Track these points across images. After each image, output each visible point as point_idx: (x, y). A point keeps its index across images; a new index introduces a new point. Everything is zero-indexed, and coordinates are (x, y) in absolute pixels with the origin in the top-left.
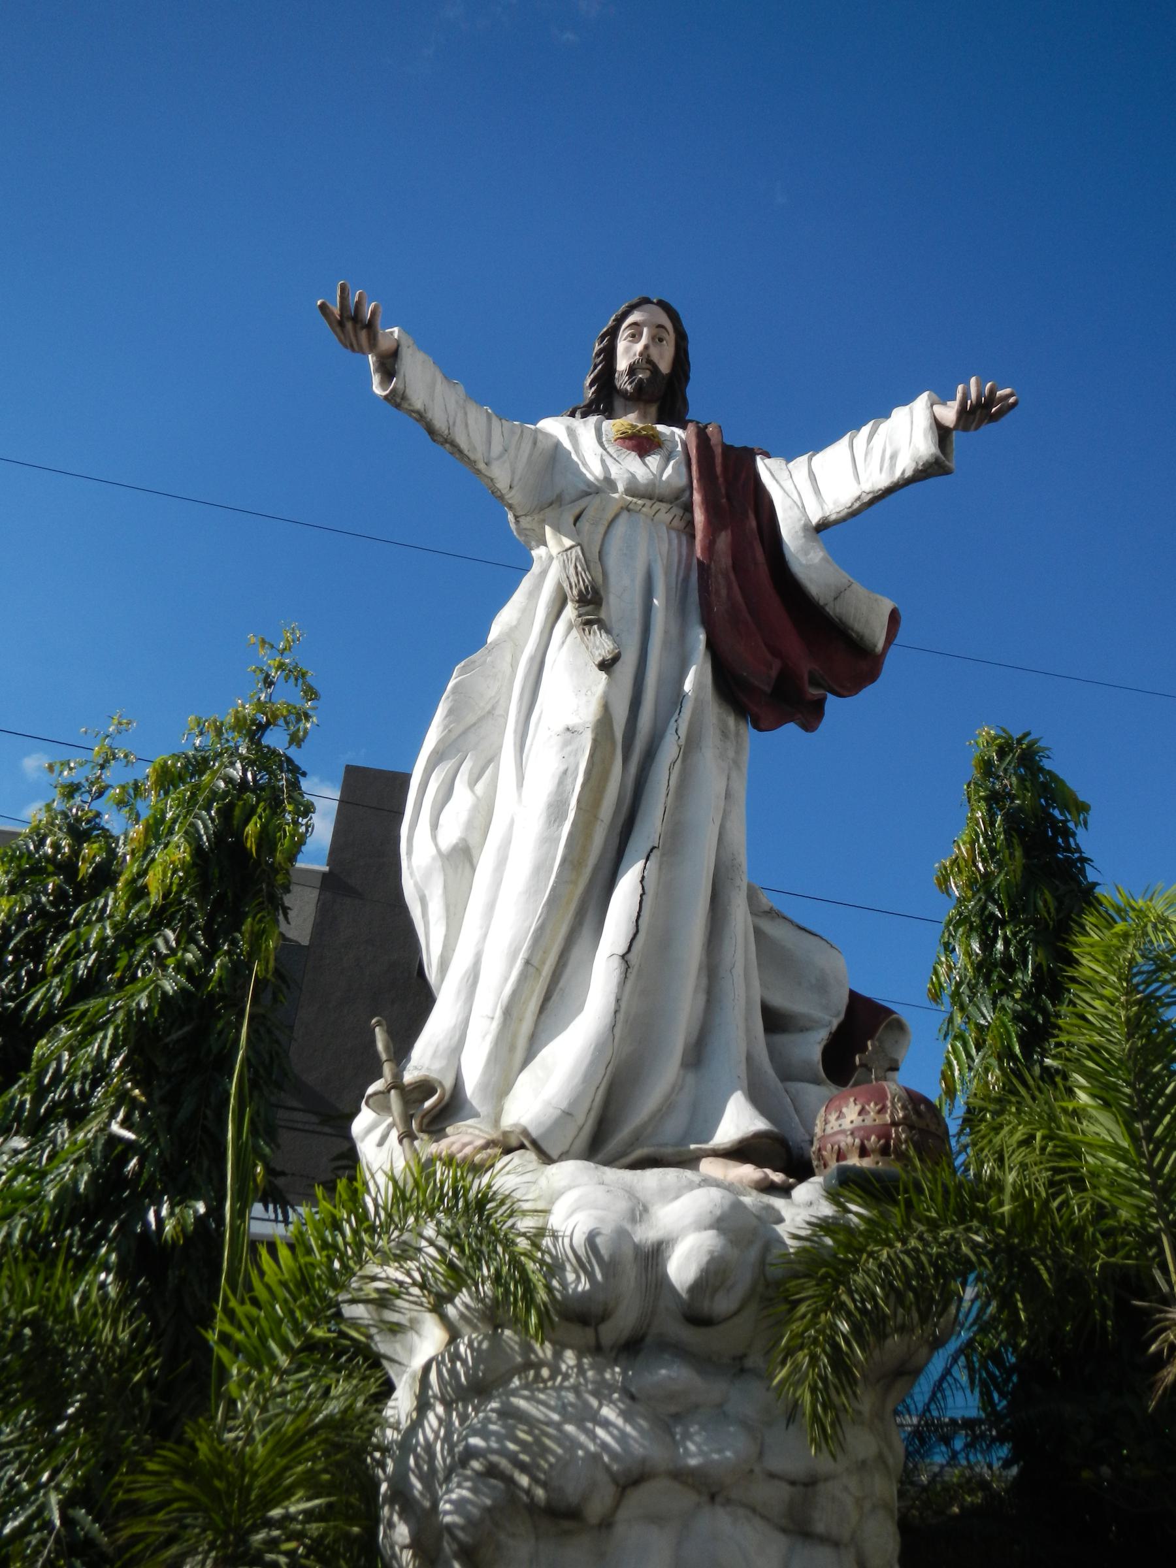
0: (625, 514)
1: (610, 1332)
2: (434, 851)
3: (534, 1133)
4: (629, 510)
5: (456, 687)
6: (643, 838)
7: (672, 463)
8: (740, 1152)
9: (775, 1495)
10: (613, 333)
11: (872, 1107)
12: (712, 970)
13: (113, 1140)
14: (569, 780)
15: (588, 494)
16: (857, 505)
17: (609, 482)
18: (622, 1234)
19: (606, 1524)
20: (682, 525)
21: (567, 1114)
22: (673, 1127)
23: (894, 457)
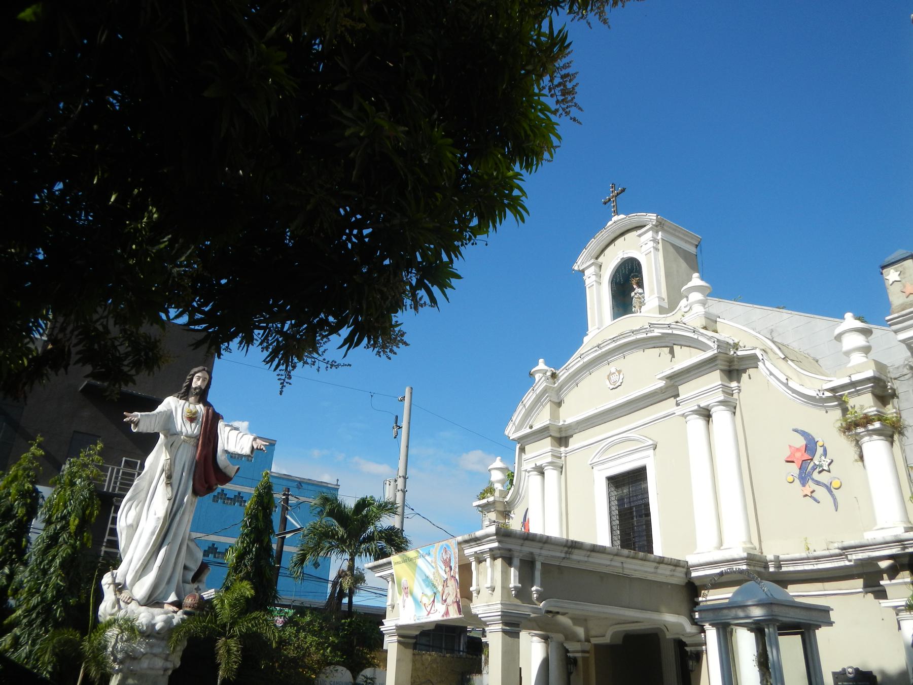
0: (183, 443)
1: (145, 635)
2: (125, 525)
3: (139, 600)
4: (184, 441)
5: (136, 485)
6: (167, 541)
7: (198, 426)
8: (173, 604)
9: (164, 656)
10: (193, 375)
11: (193, 600)
12: (175, 563)
13: (58, 584)
15: (175, 434)
17: (182, 432)
18: (150, 622)
19: (140, 659)
20: (195, 445)
21: (145, 597)
22: (162, 596)
23: (242, 449)
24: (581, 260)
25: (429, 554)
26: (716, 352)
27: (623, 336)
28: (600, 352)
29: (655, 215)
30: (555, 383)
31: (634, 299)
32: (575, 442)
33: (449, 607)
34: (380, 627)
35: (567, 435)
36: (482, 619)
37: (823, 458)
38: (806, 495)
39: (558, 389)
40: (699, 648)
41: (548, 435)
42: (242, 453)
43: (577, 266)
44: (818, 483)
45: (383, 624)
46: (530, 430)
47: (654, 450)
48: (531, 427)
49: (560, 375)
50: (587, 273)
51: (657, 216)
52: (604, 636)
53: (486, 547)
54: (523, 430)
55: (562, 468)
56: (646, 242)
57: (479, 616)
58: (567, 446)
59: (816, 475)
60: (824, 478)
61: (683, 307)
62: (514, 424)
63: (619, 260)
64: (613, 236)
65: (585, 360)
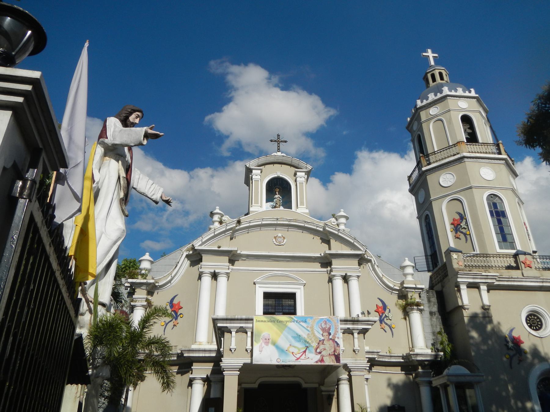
3: (108, 305)
10: (135, 111)
14: (119, 239)
16: (143, 194)
23: (154, 194)
24: (252, 163)
25: (305, 322)
26: (364, 253)
27: (296, 220)
28: (276, 222)
29: (312, 167)
30: (236, 226)
31: (276, 199)
32: (239, 266)
33: (323, 357)
34: (220, 363)
35: (235, 259)
36: (349, 367)
37: (389, 314)
38: (382, 328)
39: (235, 231)
40: (331, 393)
41: (229, 255)
42: (152, 198)
43: (249, 164)
44: (386, 324)
45: (221, 361)
46: (217, 249)
47: (304, 286)
48: (219, 247)
49: (243, 223)
50: (254, 171)
51: (312, 168)
52: (255, 383)
53: (361, 327)
54: (203, 246)
55: (229, 277)
56: (301, 177)
57: (348, 365)
58: (233, 265)
59: (385, 320)
60: (388, 322)
61: (332, 222)
62: (202, 240)
63: (276, 176)
64: (276, 161)
65: (263, 223)
